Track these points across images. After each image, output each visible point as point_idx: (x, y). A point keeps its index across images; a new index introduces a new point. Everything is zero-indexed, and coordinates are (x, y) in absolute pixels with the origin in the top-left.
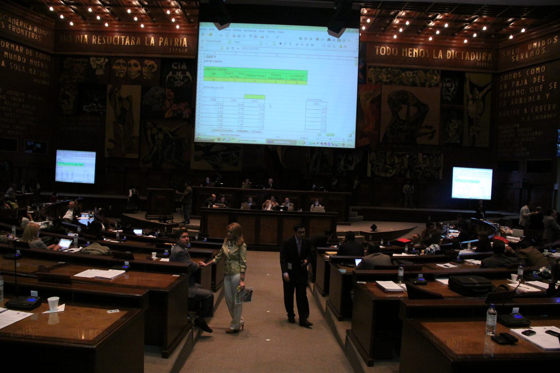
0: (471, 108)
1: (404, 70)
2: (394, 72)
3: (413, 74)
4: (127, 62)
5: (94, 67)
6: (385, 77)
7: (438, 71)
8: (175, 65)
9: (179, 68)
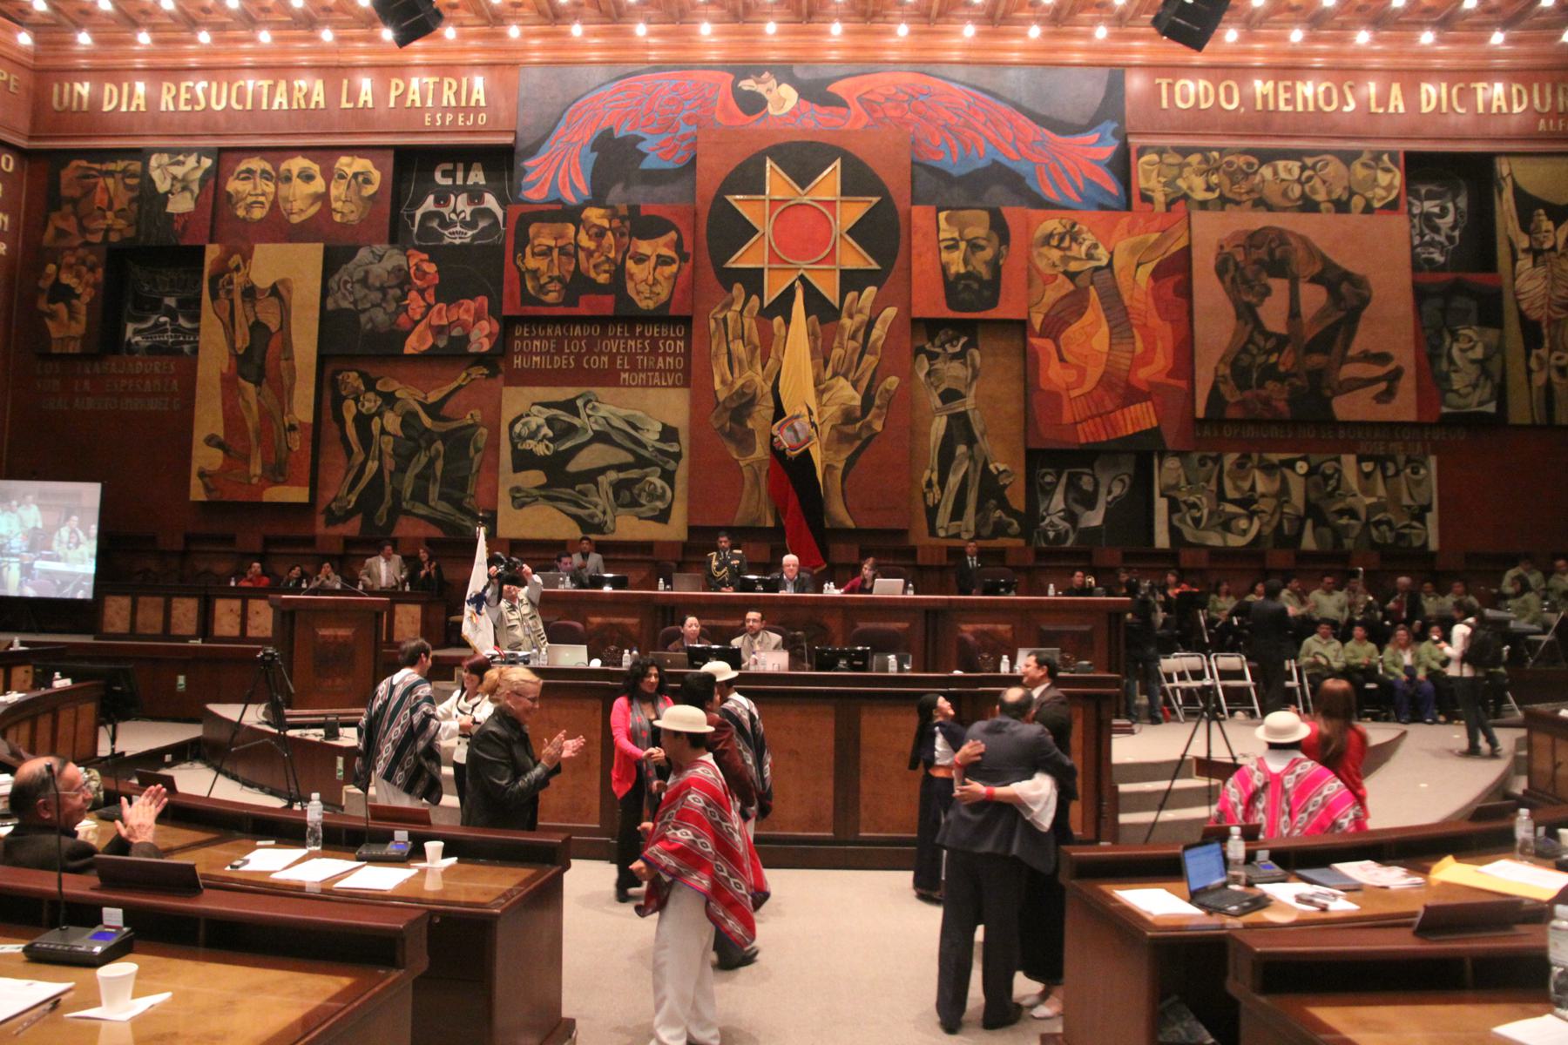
1: (1267, 157)
2: (1230, 164)
3: (1303, 168)
4: (276, 169)
5: (163, 186)
6: (1199, 182)
7: (1393, 156)
8: (445, 174)
9: (460, 182)
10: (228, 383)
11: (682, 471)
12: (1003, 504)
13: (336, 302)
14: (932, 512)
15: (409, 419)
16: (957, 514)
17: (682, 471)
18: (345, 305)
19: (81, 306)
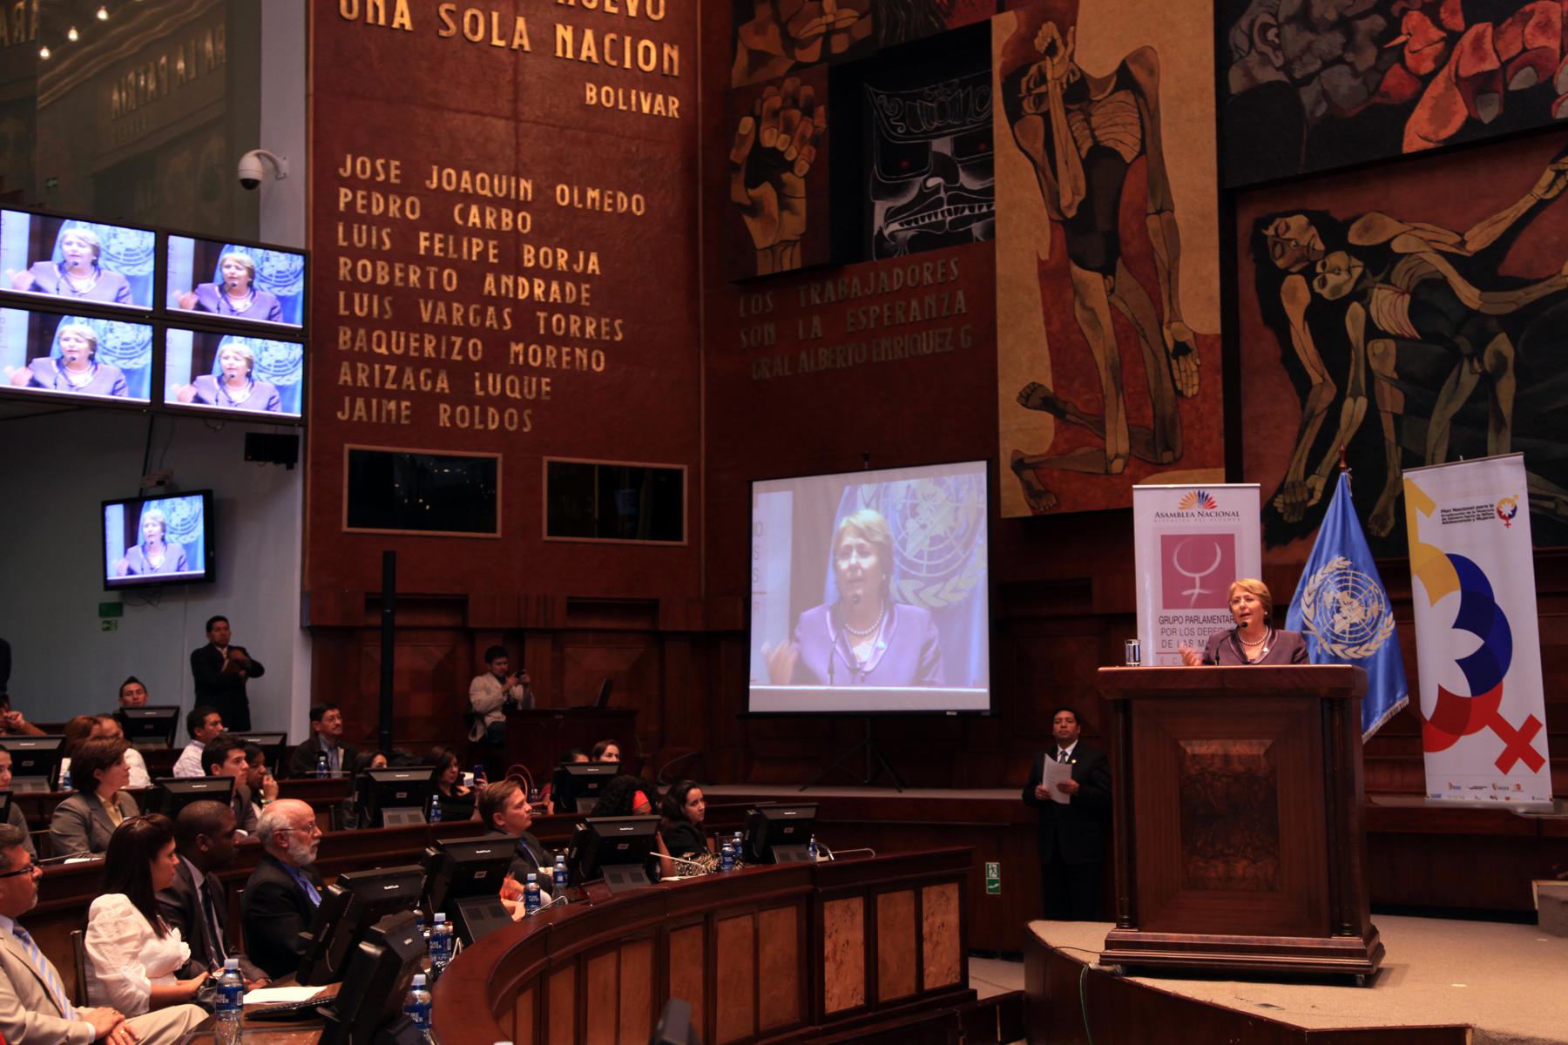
10: (1053, 278)
13: (1248, 74)
15: (1428, 298)
18: (1268, 75)
19: (796, 182)
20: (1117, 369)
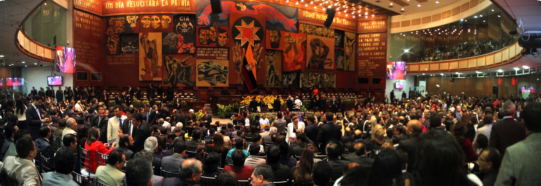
0: (347, 50)
6: (308, 30)
11: (228, 75)
12: (278, 80)
14: (267, 82)
15: (179, 65)
16: (271, 82)
17: (228, 75)
20: (152, 68)
